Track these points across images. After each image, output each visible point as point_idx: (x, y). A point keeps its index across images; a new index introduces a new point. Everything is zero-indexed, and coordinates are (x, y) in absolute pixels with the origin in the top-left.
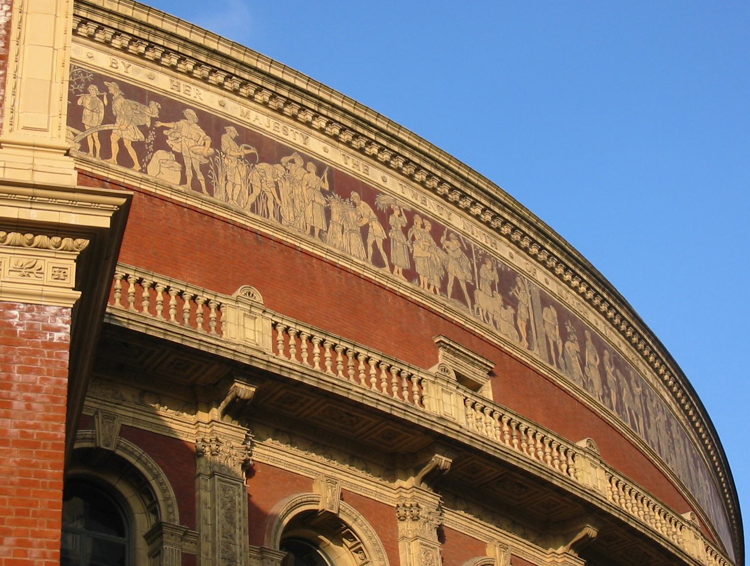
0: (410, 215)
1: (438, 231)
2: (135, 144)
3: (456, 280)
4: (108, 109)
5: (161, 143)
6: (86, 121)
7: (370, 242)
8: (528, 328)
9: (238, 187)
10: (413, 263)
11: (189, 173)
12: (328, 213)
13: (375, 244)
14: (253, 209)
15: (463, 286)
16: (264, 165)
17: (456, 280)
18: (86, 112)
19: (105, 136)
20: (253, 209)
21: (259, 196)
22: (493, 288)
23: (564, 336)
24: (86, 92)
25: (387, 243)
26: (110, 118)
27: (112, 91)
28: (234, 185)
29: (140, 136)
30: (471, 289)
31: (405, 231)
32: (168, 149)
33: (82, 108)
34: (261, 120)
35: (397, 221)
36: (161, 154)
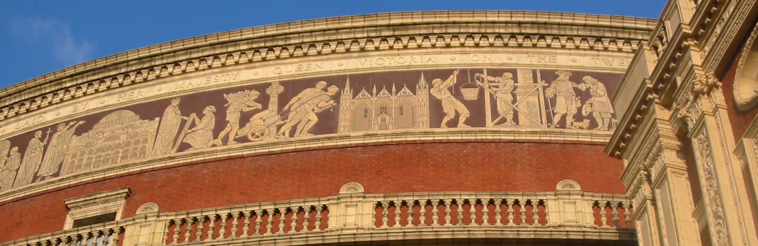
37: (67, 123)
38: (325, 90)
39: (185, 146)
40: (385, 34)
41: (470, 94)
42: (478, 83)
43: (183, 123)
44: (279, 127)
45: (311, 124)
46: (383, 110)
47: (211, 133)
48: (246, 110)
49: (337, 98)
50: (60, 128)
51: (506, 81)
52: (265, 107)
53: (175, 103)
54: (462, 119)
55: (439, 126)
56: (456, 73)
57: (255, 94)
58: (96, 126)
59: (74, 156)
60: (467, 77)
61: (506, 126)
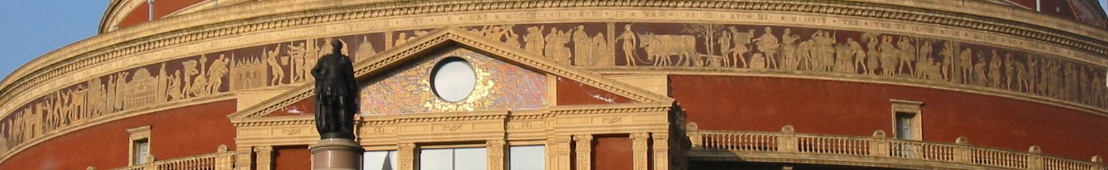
0: (880, 38)
1: (896, 39)
2: (744, 55)
3: (905, 63)
4: (731, 41)
5: (755, 51)
6: (722, 51)
7: (857, 62)
9: (791, 60)
10: (880, 63)
11: (768, 60)
12: (835, 55)
13: (859, 63)
14: (798, 68)
15: (909, 64)
16: (803, 43)
17: (905, 63)
18: (722, 46)
20: (798, 68)
21: (801, 61)
22: (928, 56)
23: (975, 61)
24: (721, 35)
26: (732, 45)
27: (732, 31)
28: (789, 59)
30: (914, 64)
31: (876, 48)
33: (720, 44)
35: (871, 45)
36: (756, 55)
37: (122, 72)
38: (224, 61)
39: (170, 98)
40: (245, 23)
41: (285, 60)
42: (289, 52)
43: (168, 80)
44: (206, 87)
45: (219, 85)
46: (248, 74)
47: (179, 89)
48: (193, 74)
49: (228, 66)
50: (120, 76)
51: (301, 49)
52: (200, 73)
53: (164, 66)
54: (281, 79)
55: (270, 85)
56: (279, 45)
57: (195, 62)
58: (133, 78)
59: (127, 98)
60: (285, 46)
61: (300, 82)
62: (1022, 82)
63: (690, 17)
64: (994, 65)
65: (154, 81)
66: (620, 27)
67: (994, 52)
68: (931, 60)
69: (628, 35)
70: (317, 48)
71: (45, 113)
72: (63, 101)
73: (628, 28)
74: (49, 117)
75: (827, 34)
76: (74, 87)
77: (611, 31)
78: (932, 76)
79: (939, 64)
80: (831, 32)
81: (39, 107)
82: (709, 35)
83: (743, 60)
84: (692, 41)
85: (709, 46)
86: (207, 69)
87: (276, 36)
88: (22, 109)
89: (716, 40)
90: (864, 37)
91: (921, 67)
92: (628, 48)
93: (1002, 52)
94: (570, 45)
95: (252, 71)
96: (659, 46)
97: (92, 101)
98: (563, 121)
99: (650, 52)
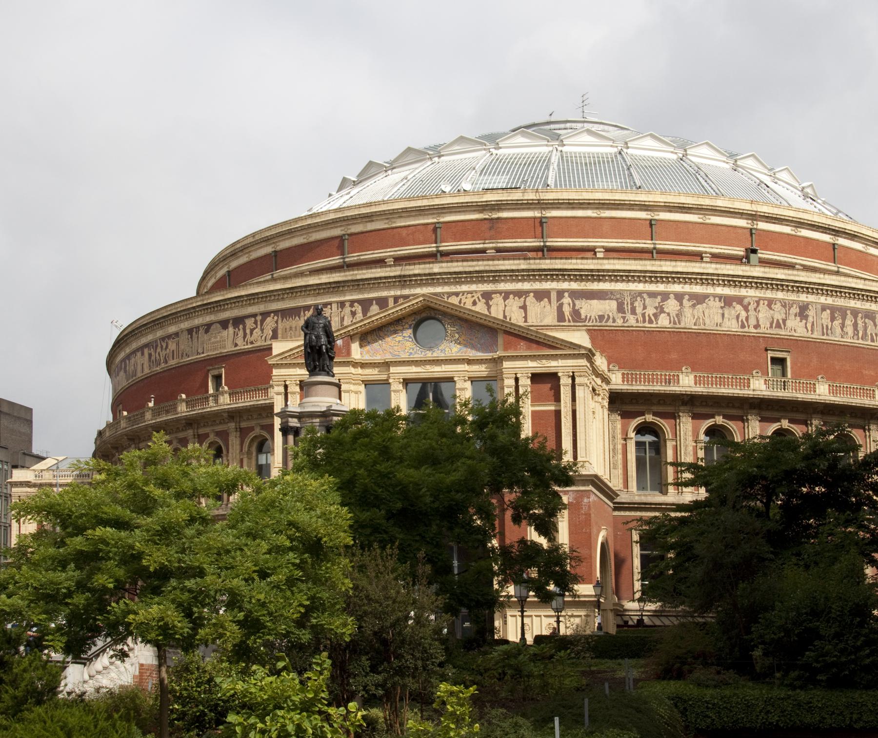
1: (770, 303)
2: (653, 315)
3: (778, 320)
4: (644, 304)
5: (662, 311)
6: (637, 311)
8: (813, 324)
10: (758, 321)
12: (723, 315)
15: (781, 321)
17: (778, 320)
19: (643, 315)
22: (796, 315)
23: (833, 319)
25: (747, 319)
26: (645, 308)
29: (655, 311)
30: (784, 321)
31: (755, 309)
32: (664, 312)
34: (698, 289)
35: (751, 307)
36: (663, 315)
49: (277, 322)
62: (871, 334)
63: (612, 288)
64: (849, 322)
65: (225, 333)
66: (560, 294)
67: (848, 312)
68: (798, 318)
69: (566, 300)
70: (340, 310)
71: (150, 355)
72: (162, 347)
73: (566, 294)
74: (153, 358)
75: (717, 299)
76: (169, 337)
77: (554, 296)
78: (799, 330)
79: (804, 321)
80: (720, 297)
81: (146, 351)
82: (628, 300)
83: (653, 318)
84: (614, 304)
85: (627, 308)
86: (262, 325)
87: (310, 301)
88: (134, 352)
89: (632, 304)
90: (746, 301)
91: (789, 323)
92: (567, 310)
93: (855, 312)
94: (524, 307)
95: (294, 326)
96: (591, 309)
97: (182, 347)
98: (506, 364)
99: (583, 313)
